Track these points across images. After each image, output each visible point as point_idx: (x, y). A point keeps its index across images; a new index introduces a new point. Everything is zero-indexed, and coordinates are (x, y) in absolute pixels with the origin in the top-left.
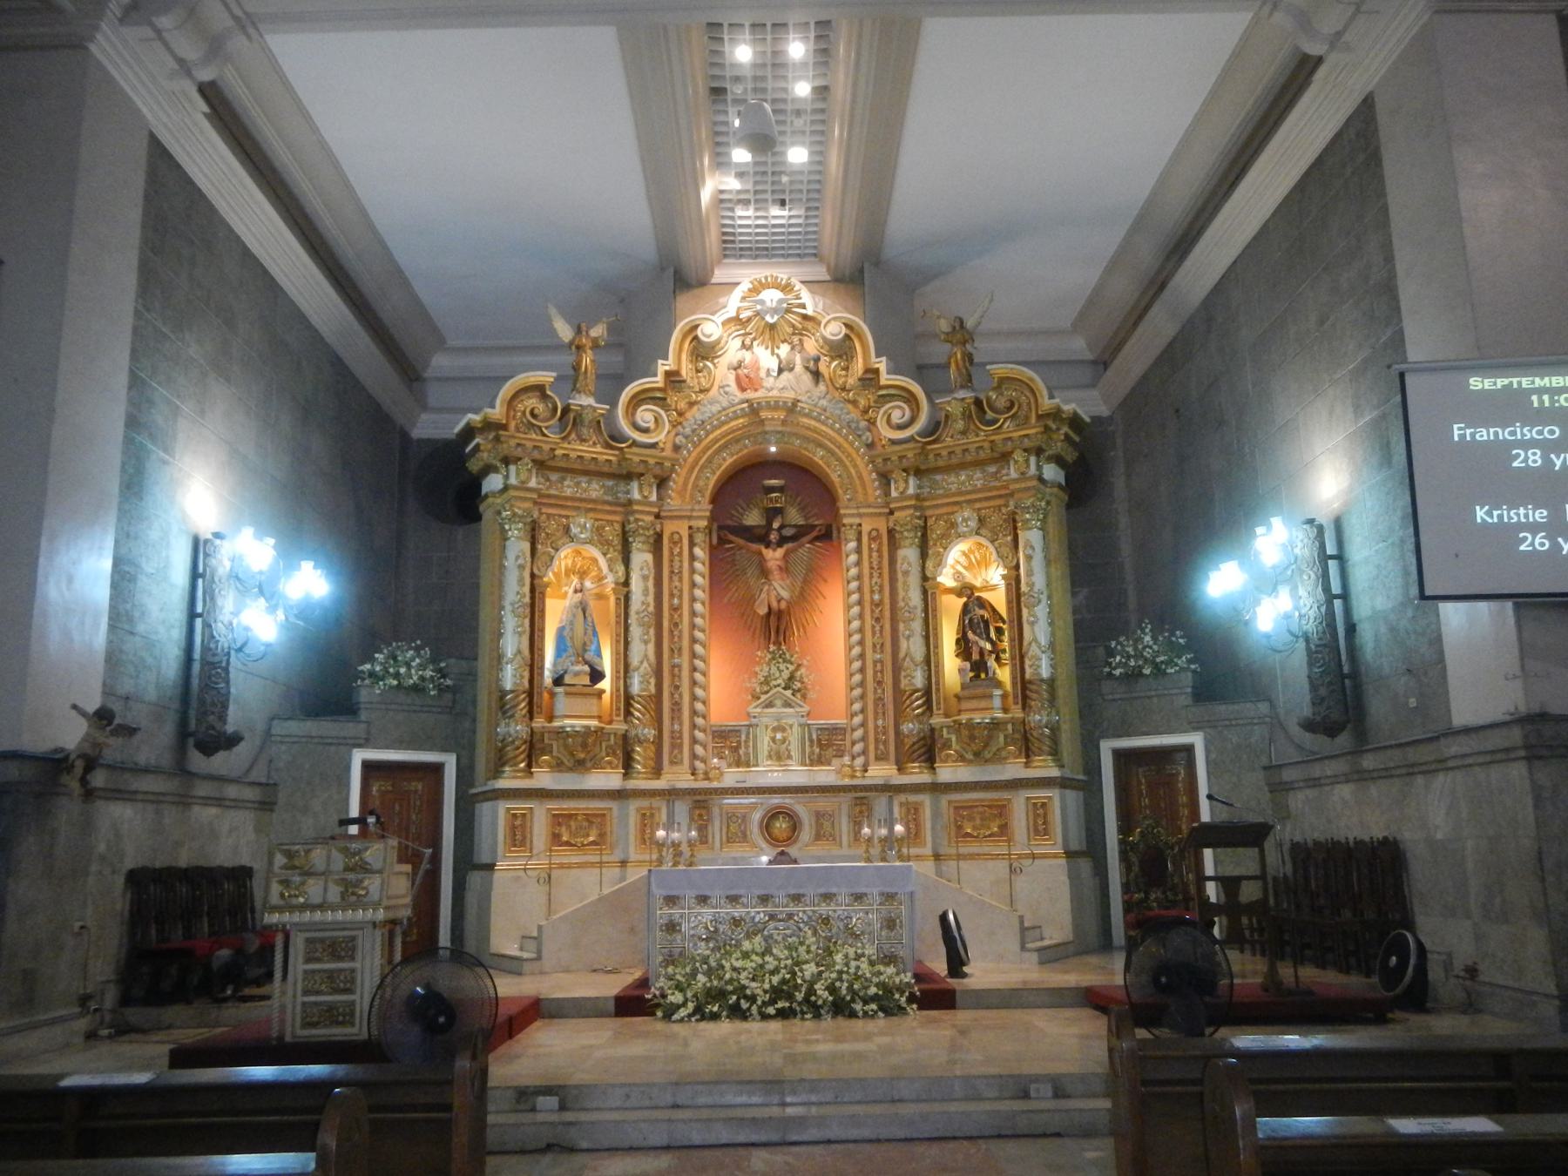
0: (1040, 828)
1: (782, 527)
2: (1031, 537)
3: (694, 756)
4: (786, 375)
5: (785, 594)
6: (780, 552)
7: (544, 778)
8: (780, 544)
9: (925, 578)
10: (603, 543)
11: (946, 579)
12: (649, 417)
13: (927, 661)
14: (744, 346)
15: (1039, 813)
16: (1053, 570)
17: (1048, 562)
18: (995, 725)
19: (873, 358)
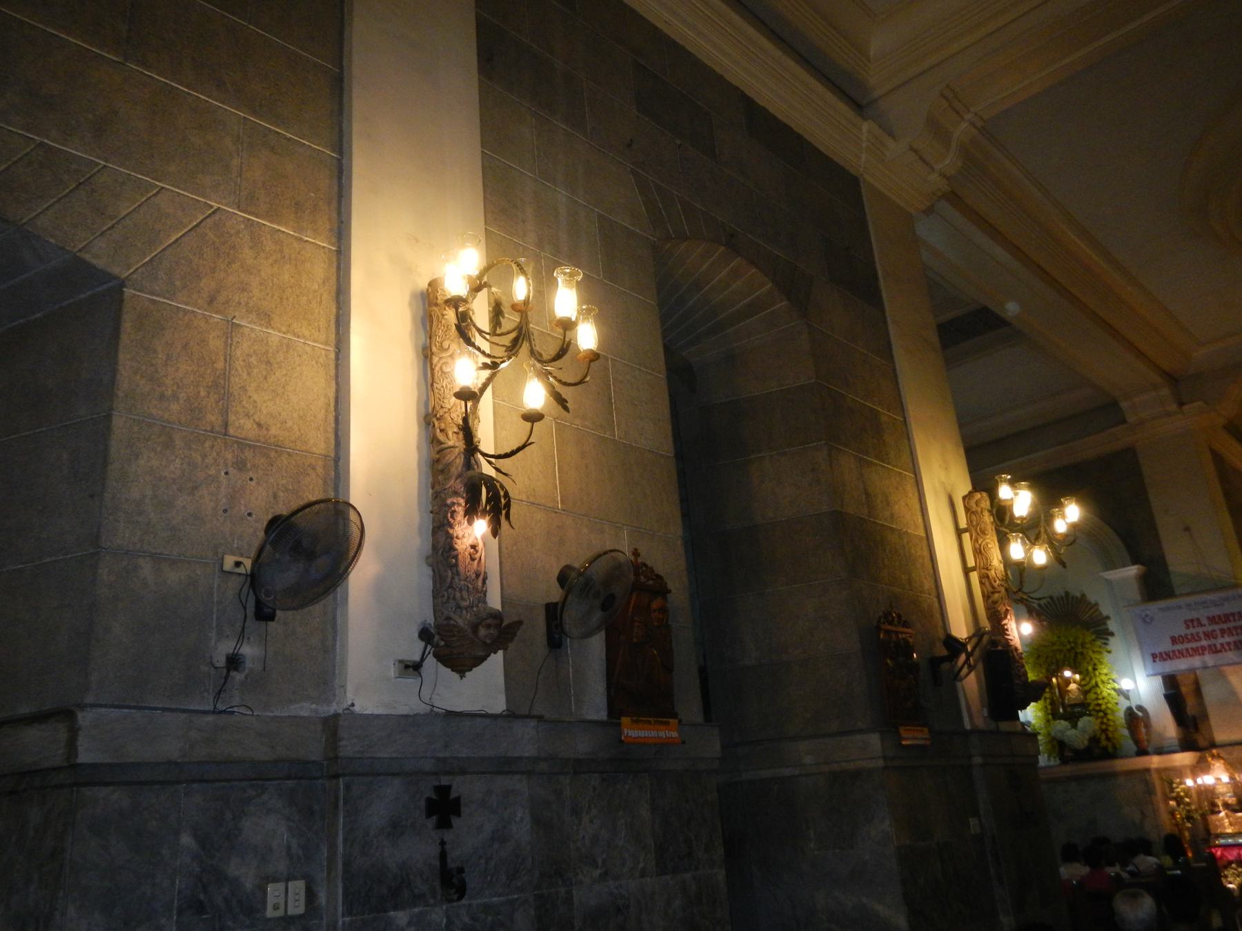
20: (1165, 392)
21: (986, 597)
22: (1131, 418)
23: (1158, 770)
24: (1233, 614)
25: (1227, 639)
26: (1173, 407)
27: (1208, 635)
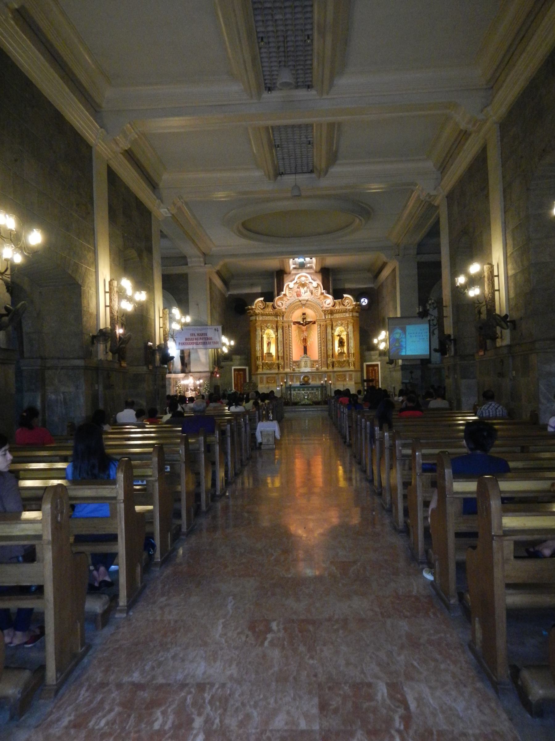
0: (351, 379)
1: (306, 322)
2: (351, 327)
3: (290, 367)
4: (306, 293)
5: (306, 335)
6: (305, 327)
7: (266, 371)
8: (305, 325)
9: (332, 334)
10: (272, 328)
11: (336, 333)
12: (281, 303)
13: (332, 349)
14: (298, 288)
15: (351, 375)
16: (355, 332)
17: (354, 331)
18: (344, 361)
19: (323, 291)
20: (202, 259)
21: (164, 335)
22: (190, 265)
23: (173, 378)
24: (204, 334)
25: (201, 341)
26: (203, 264)
27: (196, 339)
